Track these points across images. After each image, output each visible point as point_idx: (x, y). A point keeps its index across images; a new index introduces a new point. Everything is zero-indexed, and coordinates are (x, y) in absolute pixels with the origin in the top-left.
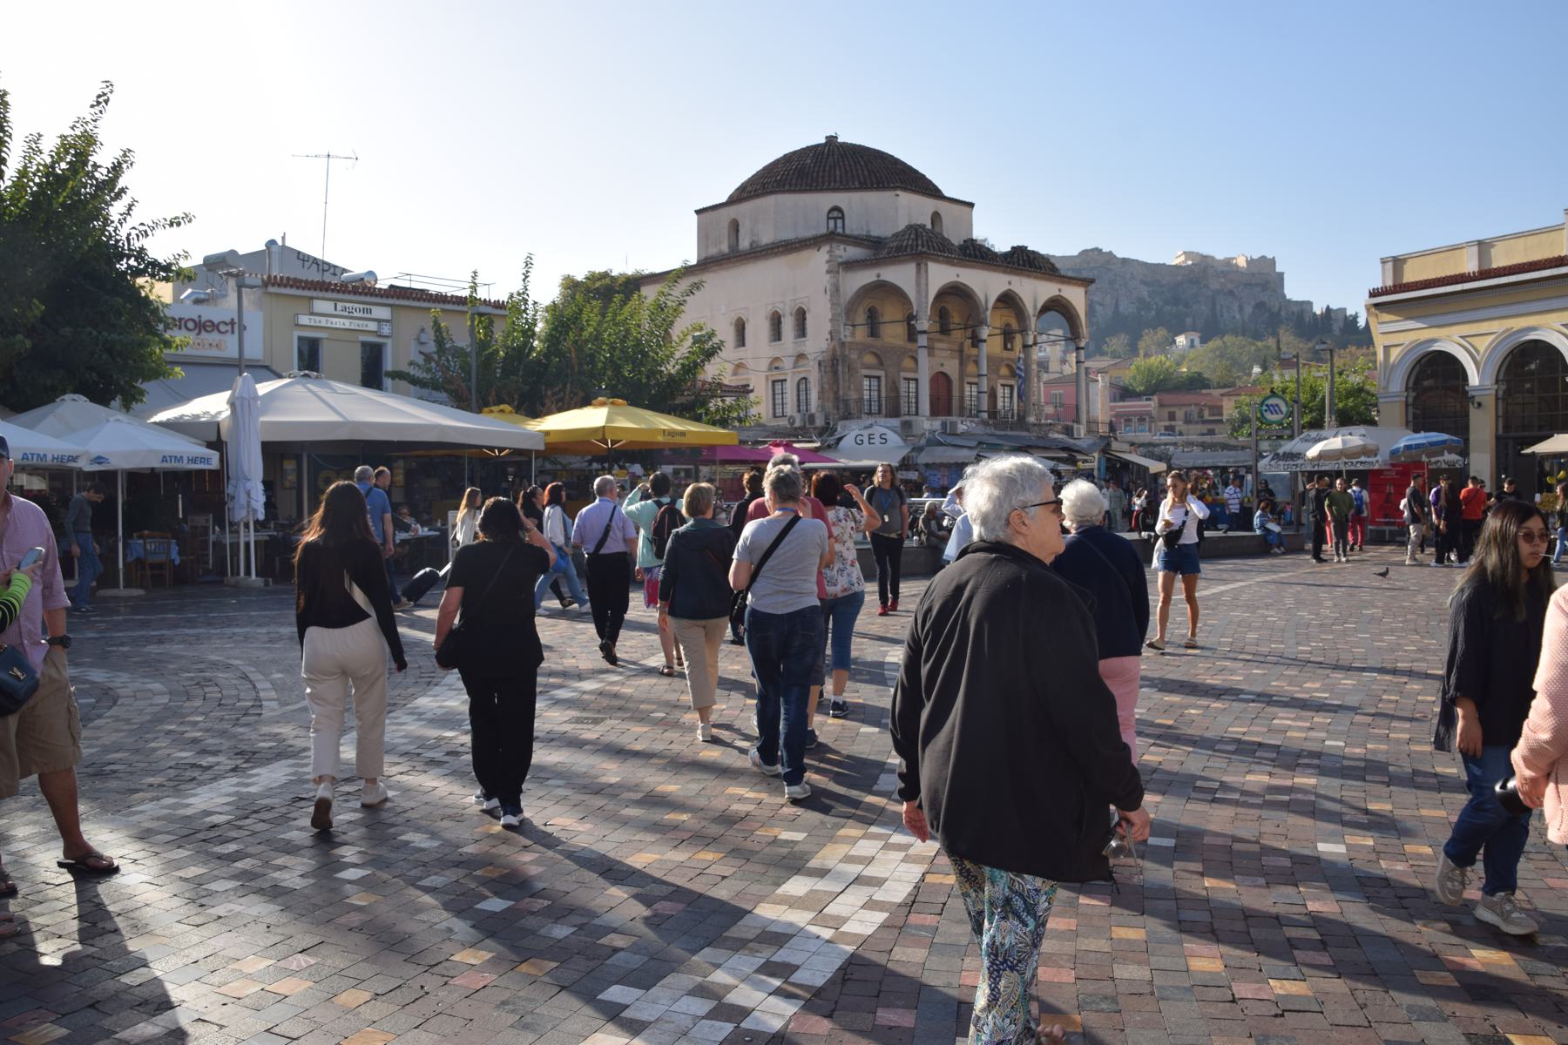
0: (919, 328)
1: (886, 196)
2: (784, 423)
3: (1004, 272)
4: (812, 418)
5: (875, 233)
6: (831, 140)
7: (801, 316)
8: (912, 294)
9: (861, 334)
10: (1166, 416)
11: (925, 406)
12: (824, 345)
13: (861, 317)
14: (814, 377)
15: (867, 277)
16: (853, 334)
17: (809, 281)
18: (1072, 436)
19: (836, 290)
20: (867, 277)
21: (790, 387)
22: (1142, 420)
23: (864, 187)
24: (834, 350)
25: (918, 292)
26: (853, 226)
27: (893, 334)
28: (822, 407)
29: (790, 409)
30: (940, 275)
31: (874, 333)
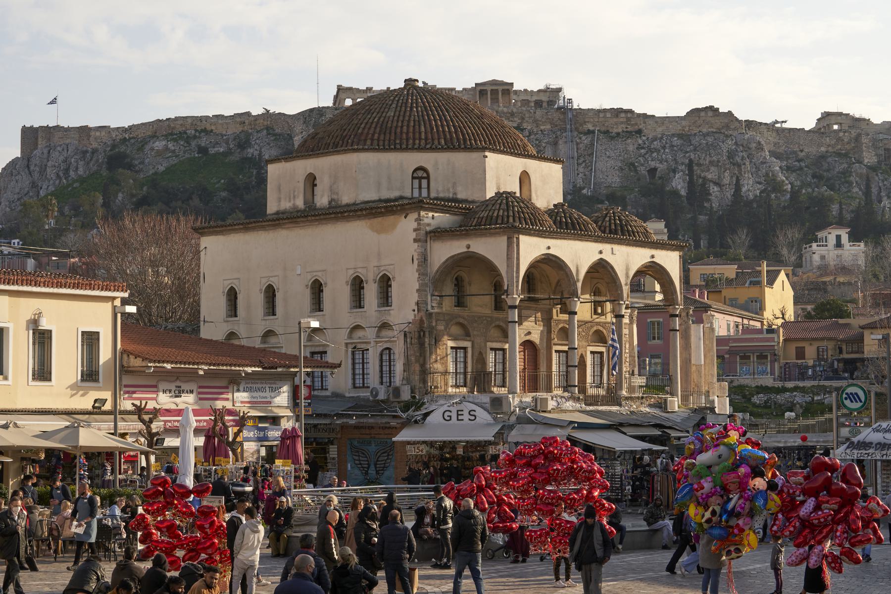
0: (510, 303)
2: (365, 394)
3: (596, 241)
4: (397, 392)
5: (460, 196)
6: (410, 83)
7: (385, 283)
8: (502, 267)
9: (448, 304)
12: (411, 317)
14: (399, 349)
16: (440, 304)
17: (396, 247)
19: (424, 260)
21: (373, 357)
23: (451, 146)
24: (422, 321)
25: (509, 266)
26: (438, 188)
27: (480, 304)
28: (407, 380)
29: (373, 380)
30: (531, 248)
31: (460, 303)
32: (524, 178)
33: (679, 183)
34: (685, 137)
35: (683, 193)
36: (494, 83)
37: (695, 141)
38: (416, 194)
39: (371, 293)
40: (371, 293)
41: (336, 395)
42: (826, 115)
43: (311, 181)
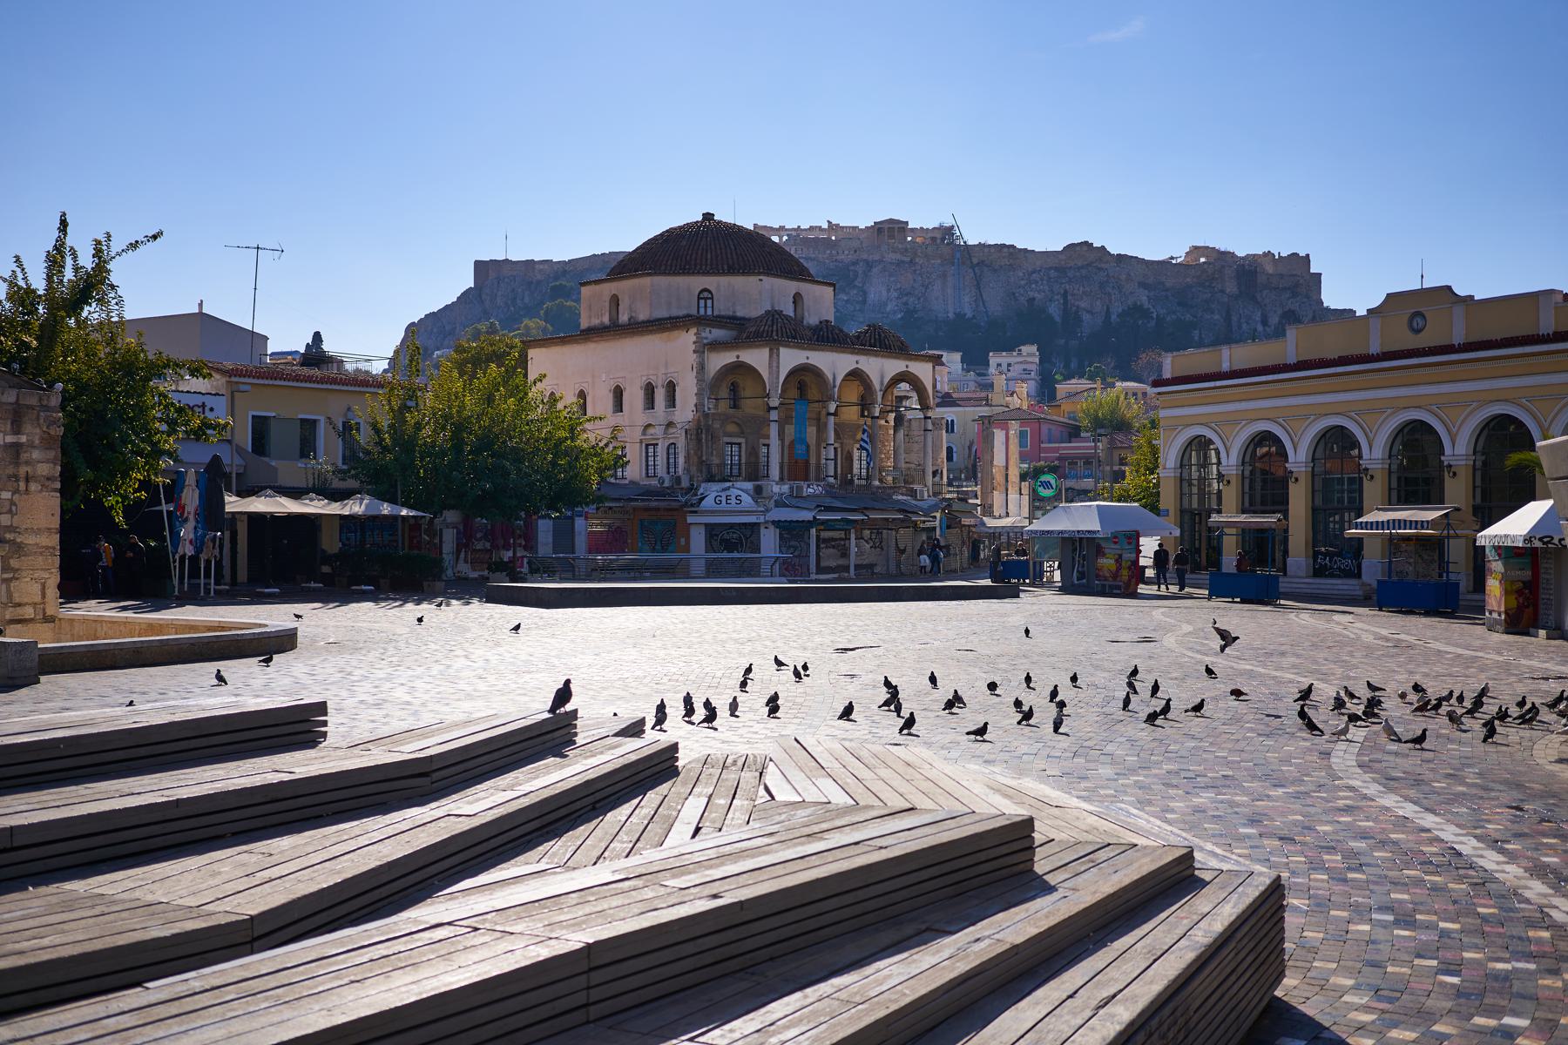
1: (753, 279)
2: (654, 482)
4: (678, 480)
5: (740, 313)
6: (708, 216)
7: (671, 388)
8: (765, 375)
9: (724, 406)
10: (1116, 459)
11: (775, 472)
13: (724, 392)
14: (681, 443)
15: (728, 357)
16: (716, 406)
17: (676, 355)
18: (915, 497)
19: (701, 367)
20: (728, 357)
21: (661, 450)
22: (1088, 462)
23: (732, 270)
26: (721, 307)
28: (687, 470)
29: (661, 470)
30: (791, 358)
32: (797, 298)
33: (1054, 310)
34: (1061, 270)
35: (1058, 319)
36: (891, 221)
37: (1070, 274)
38: (702, 311)
39: (660, 396)
40: (660, 396)
41: (632, 482)
42: (1196, 248)
43: (615, 301)
